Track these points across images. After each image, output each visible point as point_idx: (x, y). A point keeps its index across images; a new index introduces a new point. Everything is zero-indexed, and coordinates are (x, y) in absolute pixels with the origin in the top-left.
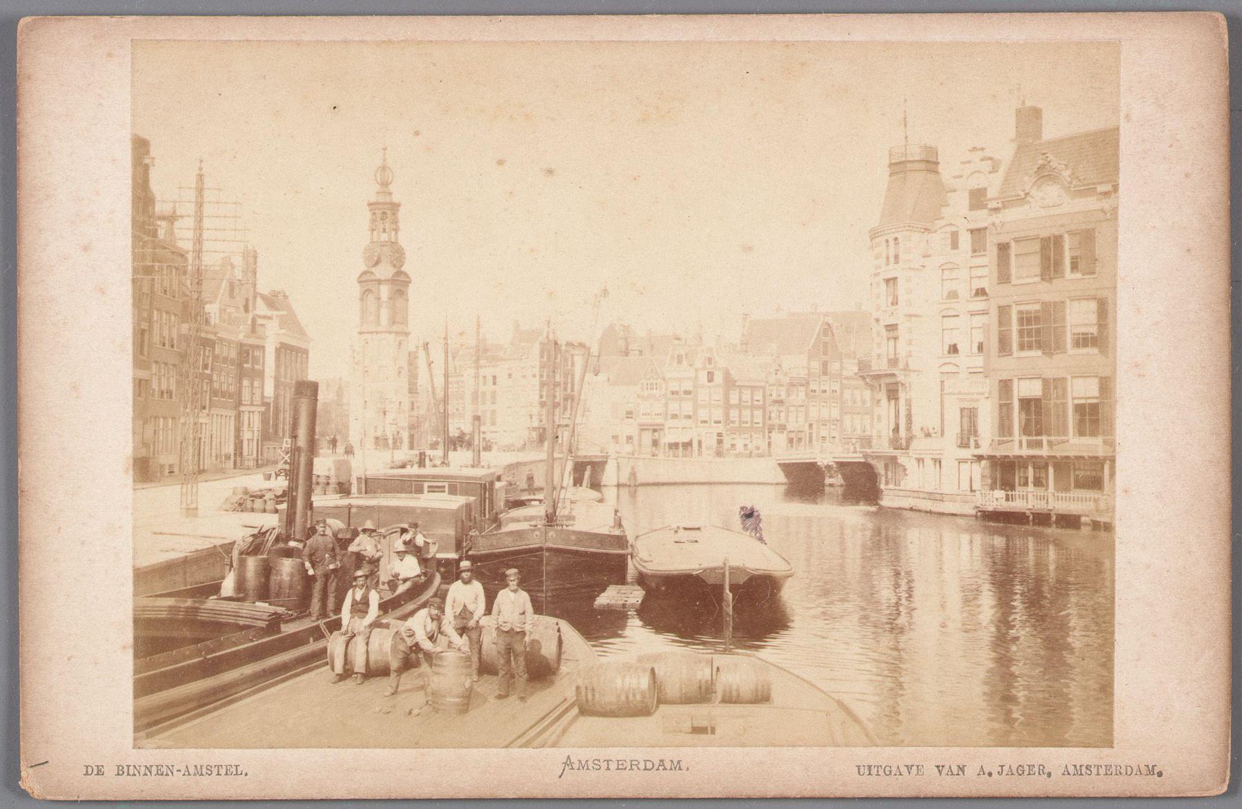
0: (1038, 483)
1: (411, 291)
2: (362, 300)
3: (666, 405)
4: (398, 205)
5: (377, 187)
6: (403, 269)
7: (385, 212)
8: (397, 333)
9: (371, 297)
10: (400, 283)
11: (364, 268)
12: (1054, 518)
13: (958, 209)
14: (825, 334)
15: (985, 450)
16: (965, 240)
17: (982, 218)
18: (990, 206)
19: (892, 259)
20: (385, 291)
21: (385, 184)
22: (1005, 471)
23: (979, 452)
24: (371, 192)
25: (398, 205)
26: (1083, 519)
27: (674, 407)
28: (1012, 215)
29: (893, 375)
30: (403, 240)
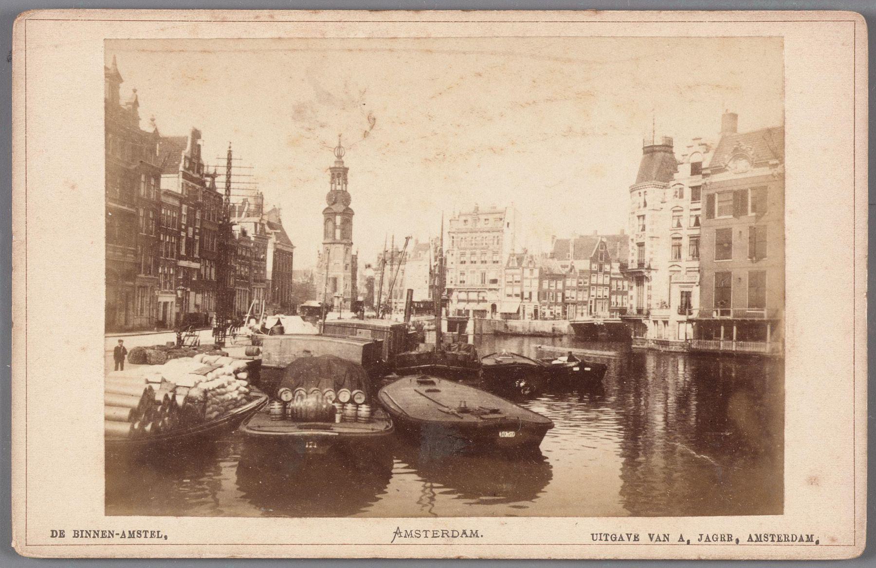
1: (355, 220)
2: (325, 224)
5: (335, 159)
8: (345, 244)
9: (330, 224)
10: (348, 215)
13: (683, 174)
14: (602, 248)
16: (688, 193)
17: (698, 180)
18: (704, 172)
20: (338, 219)
21: (339, 157)
28: (717, 178)
29: (641, 272)
30: (350, 189)
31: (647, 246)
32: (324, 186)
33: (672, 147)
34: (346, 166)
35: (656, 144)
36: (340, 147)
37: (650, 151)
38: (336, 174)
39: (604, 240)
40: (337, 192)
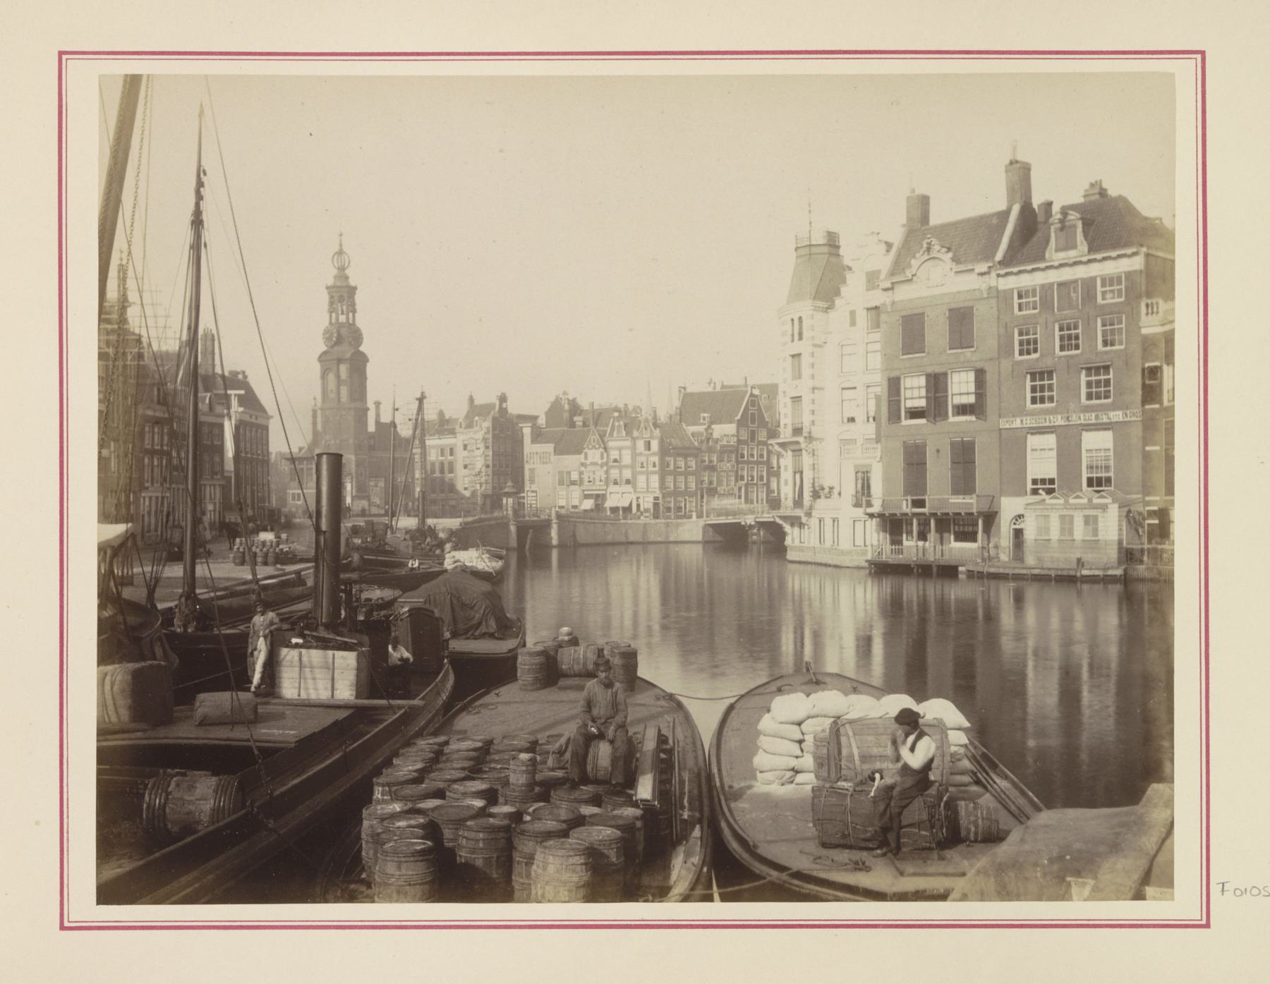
0: (923, 536)
1: (370, 369)
3: (607, 472)
4: (355, 288)
6: (361, 349)
7: (343, 295)
10: (359, 363)
11: (324, 348)
12: (935, 569)
14: (753, 405)
15: (876, 508)
16: (862, 317)
17: (878, 298)
19: (796, 336)
20: (344, 369)
21: (342, 269)
22: (894, 525)
23: (870, 510)
24: (329, 276)
25: (355, 288)
26: (961, 569)
27: (614, 473)
29: (798, 443)
30: (361, 321)
31: (806, 400)
32: (319, 319)
33: (838, 247)
34: (352, 282)
35: (813, 242)
36: (340, 252)
37: (806, 251)
38: (336, 295)
39: (756, 392)
40: (341, 325)
